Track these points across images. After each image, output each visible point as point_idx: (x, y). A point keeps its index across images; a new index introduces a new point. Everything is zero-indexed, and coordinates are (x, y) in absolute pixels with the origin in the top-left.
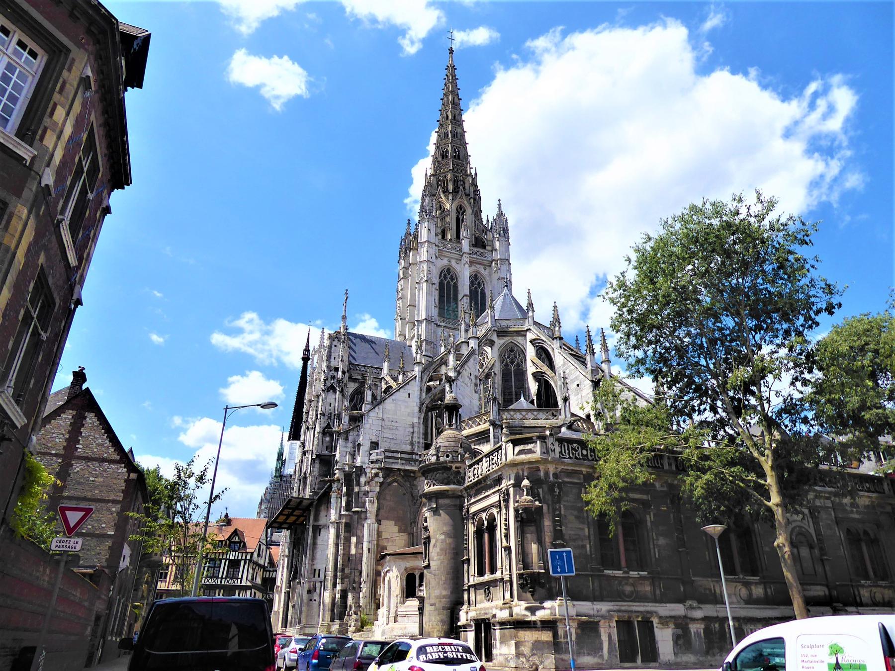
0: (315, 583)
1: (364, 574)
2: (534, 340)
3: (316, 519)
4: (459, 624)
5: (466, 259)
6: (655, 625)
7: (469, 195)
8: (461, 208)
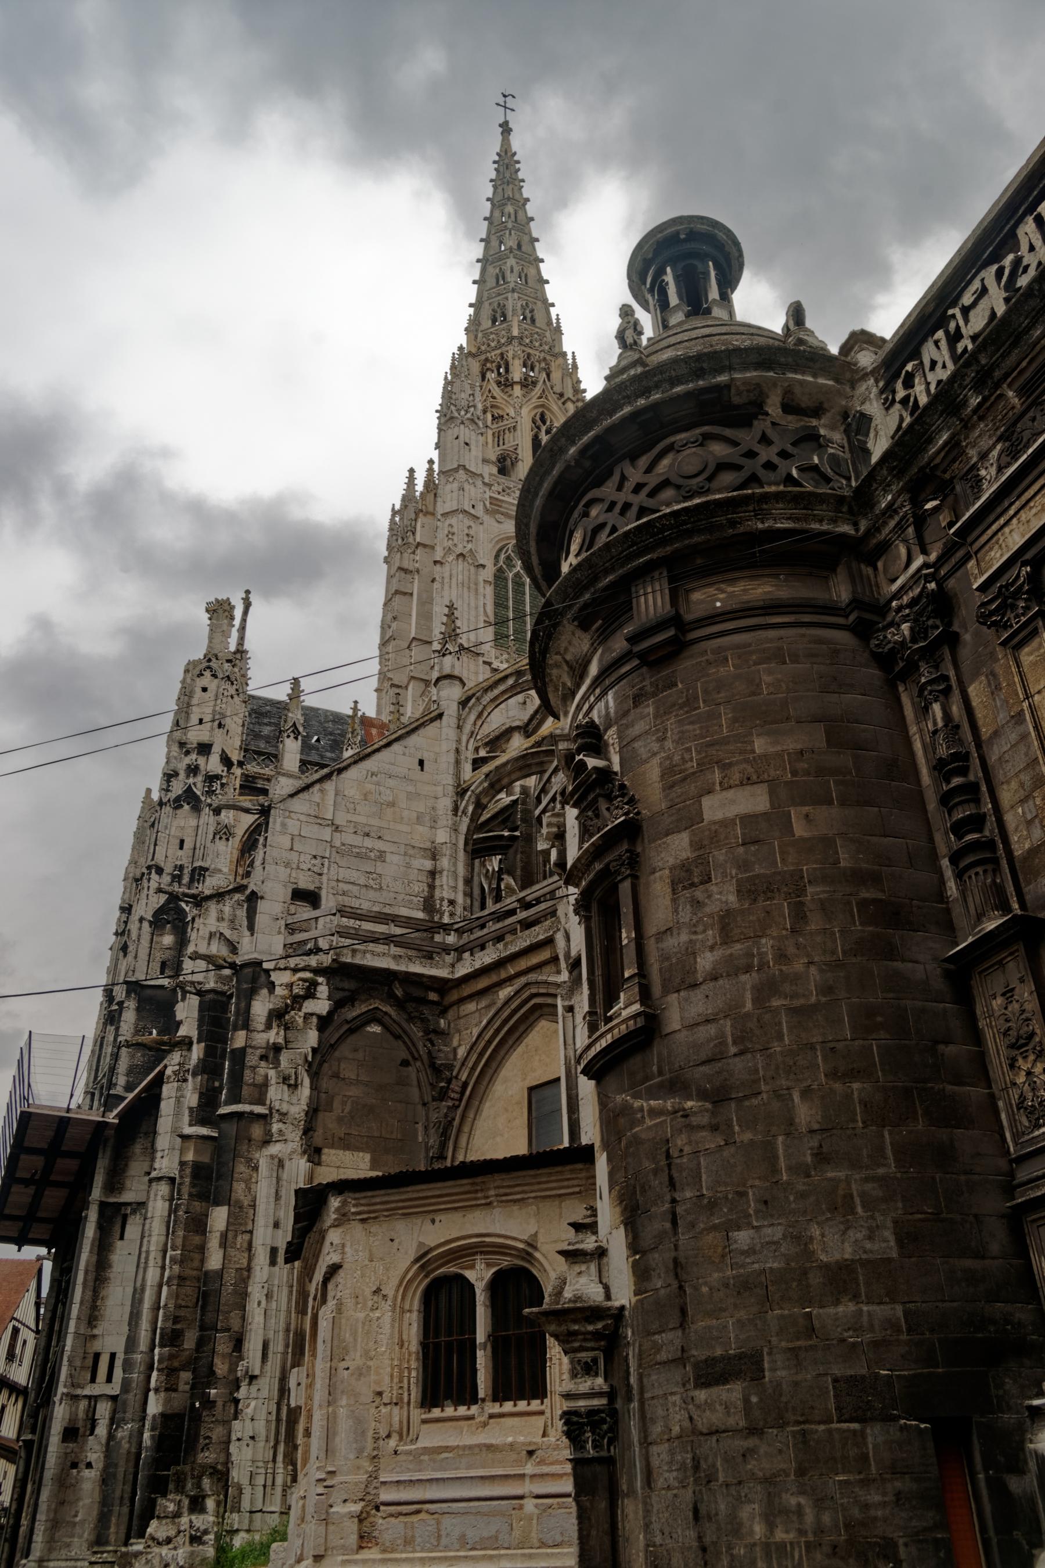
1: (253, 1347)
7: (561, 395)
8: (544, 422)
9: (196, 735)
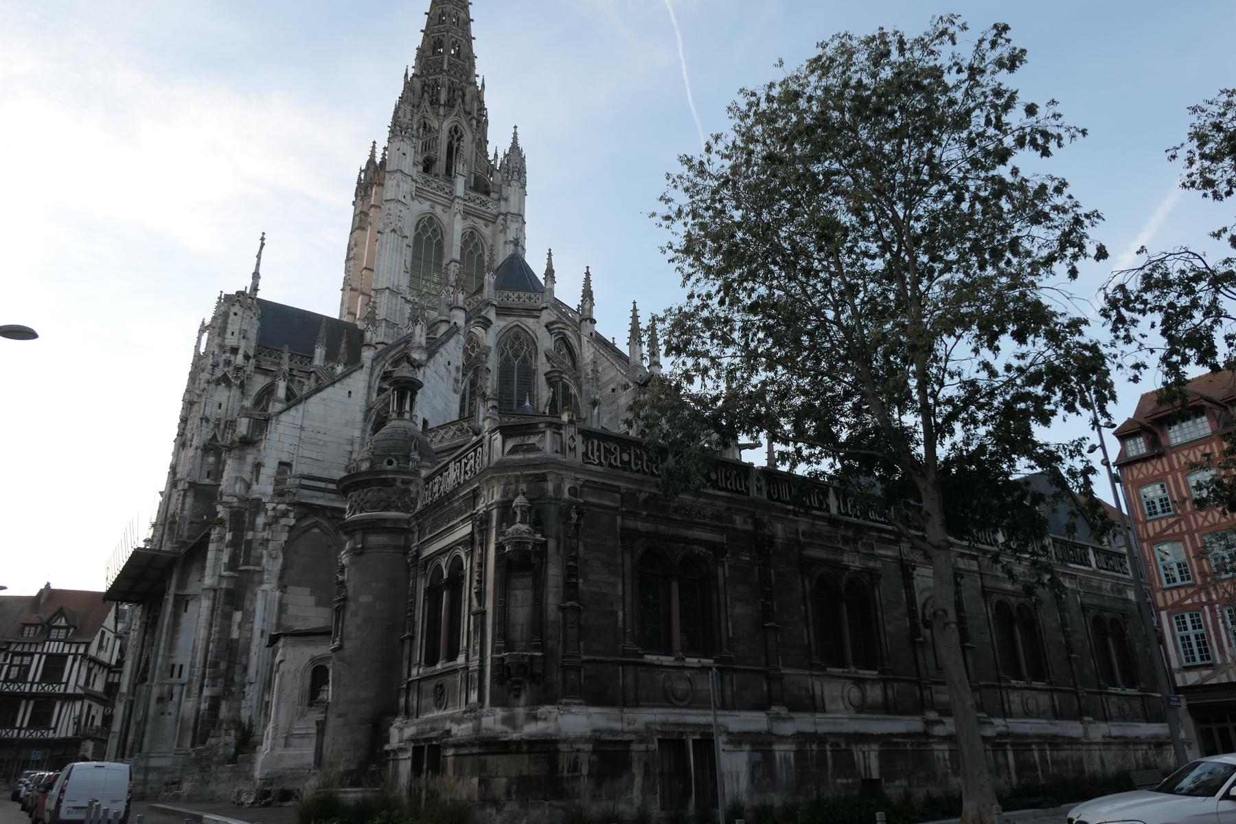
0: (172, 685)
1: (252, 671)
2: (552, 323)
3: (182, 584)
4: (387, 747)
5: (458, 206)
6: (722, 746)
7: (469, 113)
8: (456, 132)
9: (230, 341)
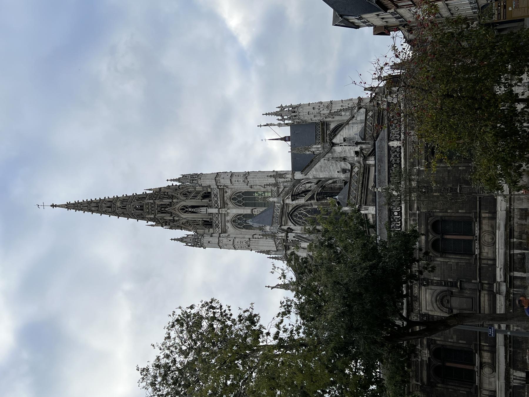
8: (183, 209)
